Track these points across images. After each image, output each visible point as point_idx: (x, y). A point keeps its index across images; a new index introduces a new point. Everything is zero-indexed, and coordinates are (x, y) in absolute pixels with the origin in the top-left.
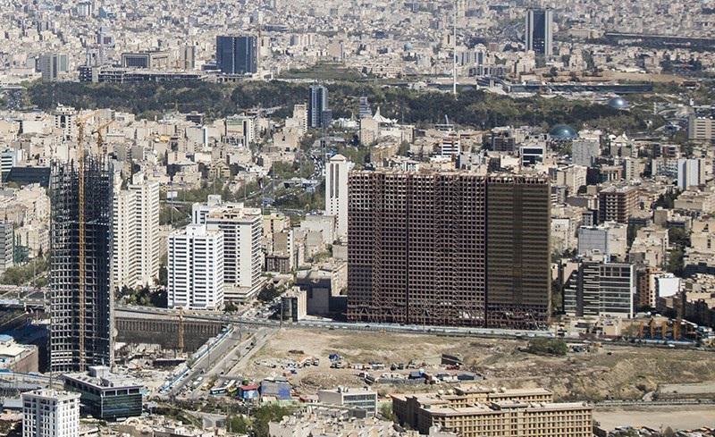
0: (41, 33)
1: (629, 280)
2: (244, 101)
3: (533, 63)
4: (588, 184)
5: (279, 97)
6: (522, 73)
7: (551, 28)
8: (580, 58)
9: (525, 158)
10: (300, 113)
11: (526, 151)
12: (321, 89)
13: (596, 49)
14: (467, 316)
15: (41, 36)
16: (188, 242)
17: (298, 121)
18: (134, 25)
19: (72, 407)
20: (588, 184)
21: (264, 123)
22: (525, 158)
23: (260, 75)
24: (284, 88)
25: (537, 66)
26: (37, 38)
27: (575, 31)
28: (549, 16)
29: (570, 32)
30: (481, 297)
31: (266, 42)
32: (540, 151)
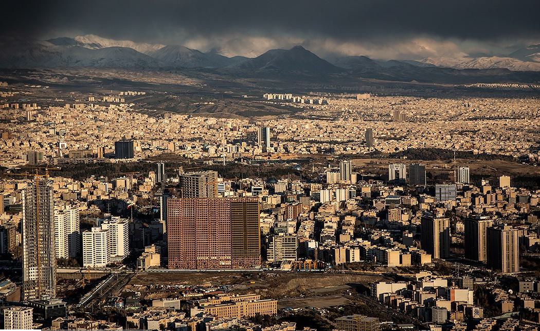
0: (31, 143)
1: (295, 244)
2: (125, 170)
3: (261, 151)
4: (411, 253)
5: (142, 169)
6: (255, 155)
7: (269, 135)
8: (282, 148)
9: (255, 192)
10: (152, 175)
11: (254, 189)
12: (162, 165)
13: (289, 143)
14: (223, 264)
15: (30, 145)
16: (92, 235)
17: (150, 181)
18: (75, 138)
19: (29, 314)
20: (411, 253)
21: (135, 181)
22: (255, 192)
23: (135, 159)
24: (146, 165)
25: (263, 152)
26: (29, 145)
27: (281, 137)
28: (268, 130)
29: (278, 137)
30: (229, 254)
31: (139, 144)
32: (261, 189)
